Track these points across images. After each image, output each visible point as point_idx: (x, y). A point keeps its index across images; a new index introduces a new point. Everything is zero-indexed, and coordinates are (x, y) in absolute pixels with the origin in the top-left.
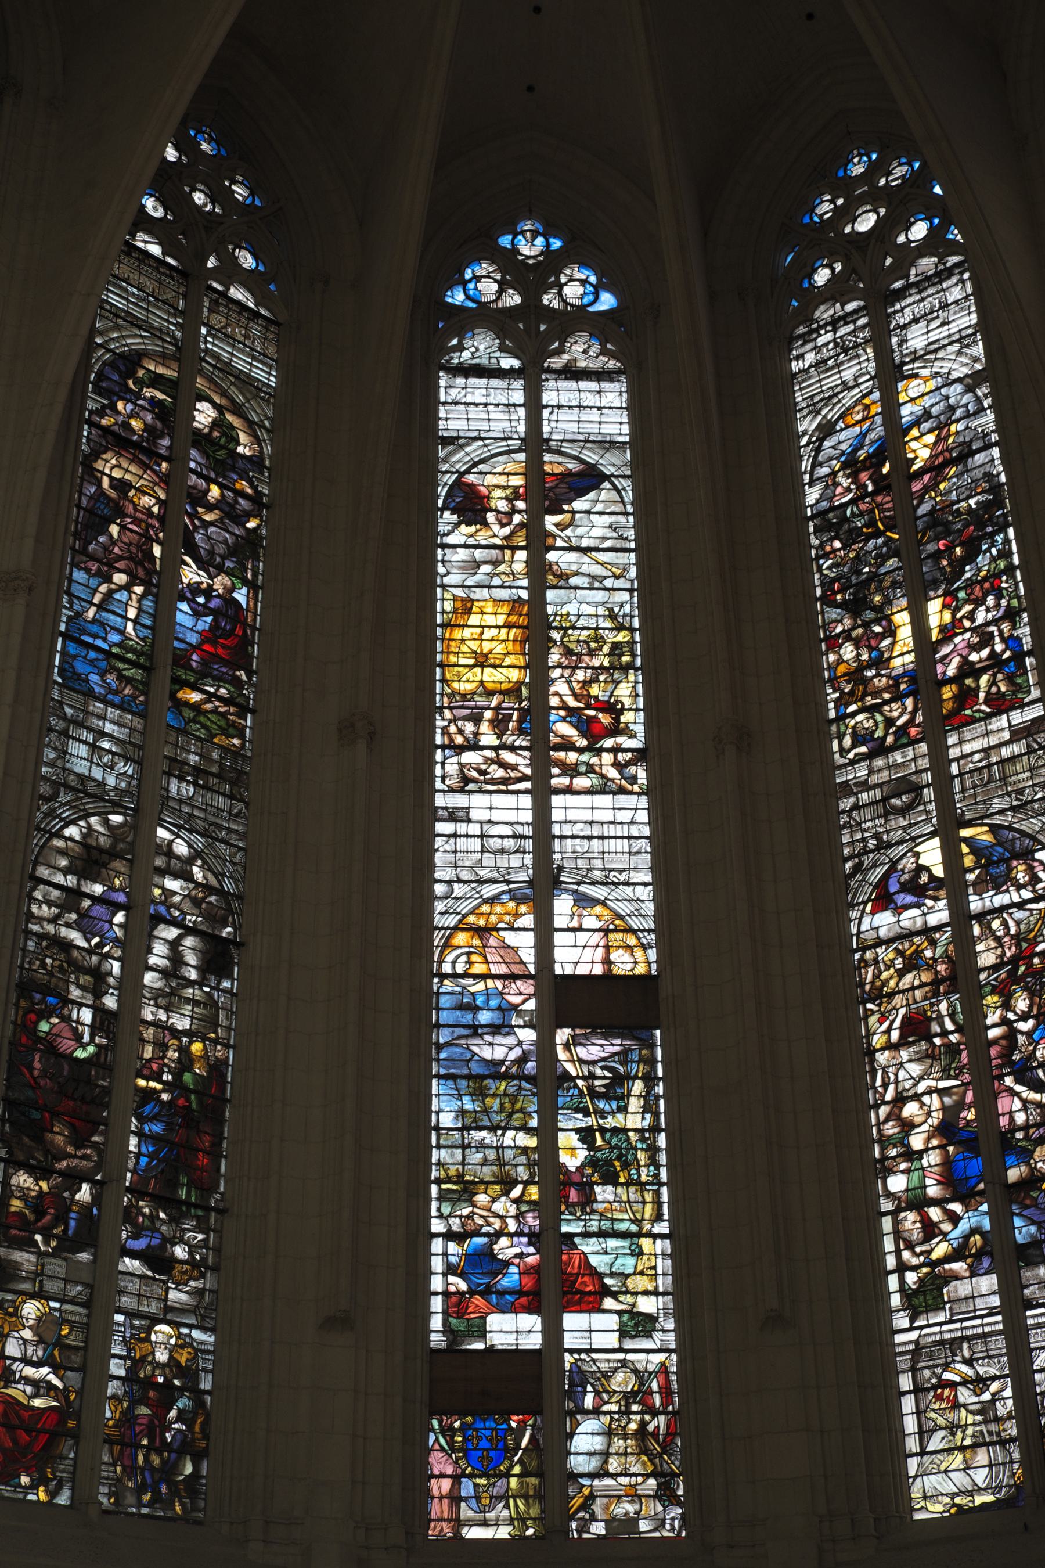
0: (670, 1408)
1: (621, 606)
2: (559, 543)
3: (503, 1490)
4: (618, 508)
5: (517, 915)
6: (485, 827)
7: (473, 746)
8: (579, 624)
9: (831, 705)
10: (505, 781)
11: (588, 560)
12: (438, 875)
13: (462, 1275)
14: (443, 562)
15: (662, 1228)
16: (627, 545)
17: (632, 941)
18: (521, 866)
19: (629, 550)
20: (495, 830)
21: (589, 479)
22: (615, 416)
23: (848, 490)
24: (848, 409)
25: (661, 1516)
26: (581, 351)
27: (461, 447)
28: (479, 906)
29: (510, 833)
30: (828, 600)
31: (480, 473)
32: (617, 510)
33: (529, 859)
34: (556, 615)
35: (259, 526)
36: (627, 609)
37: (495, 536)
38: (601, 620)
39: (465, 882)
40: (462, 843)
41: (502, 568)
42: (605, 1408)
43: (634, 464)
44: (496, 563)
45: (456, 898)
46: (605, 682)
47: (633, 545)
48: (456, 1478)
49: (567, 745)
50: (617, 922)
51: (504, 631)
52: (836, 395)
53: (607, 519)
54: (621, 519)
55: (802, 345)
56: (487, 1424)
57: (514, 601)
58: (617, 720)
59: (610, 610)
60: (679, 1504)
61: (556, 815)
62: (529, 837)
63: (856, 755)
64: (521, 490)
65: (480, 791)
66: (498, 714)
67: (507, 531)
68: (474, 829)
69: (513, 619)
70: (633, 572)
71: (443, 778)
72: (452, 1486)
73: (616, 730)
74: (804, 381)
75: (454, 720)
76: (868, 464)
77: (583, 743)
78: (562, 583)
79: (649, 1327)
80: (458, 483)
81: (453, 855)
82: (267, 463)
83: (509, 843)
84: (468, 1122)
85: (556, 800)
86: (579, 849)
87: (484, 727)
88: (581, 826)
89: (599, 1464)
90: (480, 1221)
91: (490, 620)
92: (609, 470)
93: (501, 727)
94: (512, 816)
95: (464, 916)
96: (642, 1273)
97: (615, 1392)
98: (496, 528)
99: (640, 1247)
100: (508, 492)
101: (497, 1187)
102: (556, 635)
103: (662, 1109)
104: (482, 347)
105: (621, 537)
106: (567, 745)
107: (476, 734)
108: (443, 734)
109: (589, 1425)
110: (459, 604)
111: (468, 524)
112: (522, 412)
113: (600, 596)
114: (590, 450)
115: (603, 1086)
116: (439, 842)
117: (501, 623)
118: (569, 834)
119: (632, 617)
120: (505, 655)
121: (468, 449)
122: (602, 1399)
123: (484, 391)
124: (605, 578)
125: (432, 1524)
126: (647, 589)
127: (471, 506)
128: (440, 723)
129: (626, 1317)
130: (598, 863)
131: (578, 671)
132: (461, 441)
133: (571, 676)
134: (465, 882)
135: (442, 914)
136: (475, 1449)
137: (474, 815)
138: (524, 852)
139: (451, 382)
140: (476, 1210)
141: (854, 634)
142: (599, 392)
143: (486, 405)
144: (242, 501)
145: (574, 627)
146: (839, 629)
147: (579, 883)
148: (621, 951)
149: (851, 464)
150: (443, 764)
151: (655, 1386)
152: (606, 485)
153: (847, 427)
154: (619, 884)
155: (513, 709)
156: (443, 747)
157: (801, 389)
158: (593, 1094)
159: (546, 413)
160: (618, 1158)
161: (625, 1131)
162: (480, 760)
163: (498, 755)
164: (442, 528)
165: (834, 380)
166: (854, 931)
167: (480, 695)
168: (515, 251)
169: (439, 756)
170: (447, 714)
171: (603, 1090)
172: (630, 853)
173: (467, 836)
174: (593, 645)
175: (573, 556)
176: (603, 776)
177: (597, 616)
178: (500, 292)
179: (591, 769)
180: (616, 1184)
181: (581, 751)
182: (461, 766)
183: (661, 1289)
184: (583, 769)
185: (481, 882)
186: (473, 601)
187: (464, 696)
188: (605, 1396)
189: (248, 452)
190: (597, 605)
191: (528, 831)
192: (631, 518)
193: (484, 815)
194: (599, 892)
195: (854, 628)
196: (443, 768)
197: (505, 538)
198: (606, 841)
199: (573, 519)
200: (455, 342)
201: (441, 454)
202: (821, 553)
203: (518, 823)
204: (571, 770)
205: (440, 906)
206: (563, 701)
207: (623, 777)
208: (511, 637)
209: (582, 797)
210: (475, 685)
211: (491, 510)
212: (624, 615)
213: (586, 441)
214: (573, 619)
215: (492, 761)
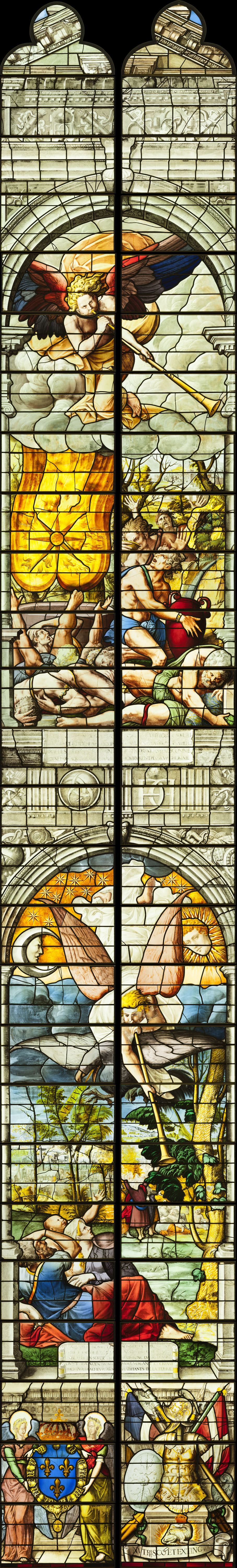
0: (226, 1438)
1: (214, 459)
3: (75, 1518)
4: (216, 303)
6: (61, 773)
11: (175, 388)
13: (35, 1303)
15: (226, 1251)
17: (208, 918)
25: (210, 1542)
39: (38, 846)
40: (34, 796)
42: (161, 1438)
48: (30, 1506)
49: (145, 662)
54: (217, 320)
56: (59, 1453)
58: (202, 624)
60: (228, 1531)
65: (55, 727)
68: (48, 776)
72: (26, 1513)
73: (200, 639)
79: (209, 1356)
80: (28, 267)
84: (41, 1134)
89: (153, 1493)
90: (51, 1244)
92: (205, 242)
95: (37, 889)
96: (204, 1300)
97: (172, 1422)
99: (203, 1273)
101: (71, 1208)
103: (233, 1119)
107: (51, 647)
109: (144, 1455)
111: (41, 336)
113: (188, 444)
115: (172, 1092)
117: (80, 487)
121: (40, 212)
122: (158, 1429)
125: (7, 1549)
129: (185, 1347)
134: (38, 846)
136: (47, 1477)
140: (48, 1233)
148: (195, 932)
151: (211, 1417)
152: (202, 268)
154: (196, 846)
158: (161, 1102)
160: (184, 1175)
161: (191, 1144)
171: (171, 1097)
174: (178, 517)
180: (181, 1203)
182: (34, 692)
183: (222, 1317)
185: (56, 846)
188: (162, 1426)
204: (146, 697)
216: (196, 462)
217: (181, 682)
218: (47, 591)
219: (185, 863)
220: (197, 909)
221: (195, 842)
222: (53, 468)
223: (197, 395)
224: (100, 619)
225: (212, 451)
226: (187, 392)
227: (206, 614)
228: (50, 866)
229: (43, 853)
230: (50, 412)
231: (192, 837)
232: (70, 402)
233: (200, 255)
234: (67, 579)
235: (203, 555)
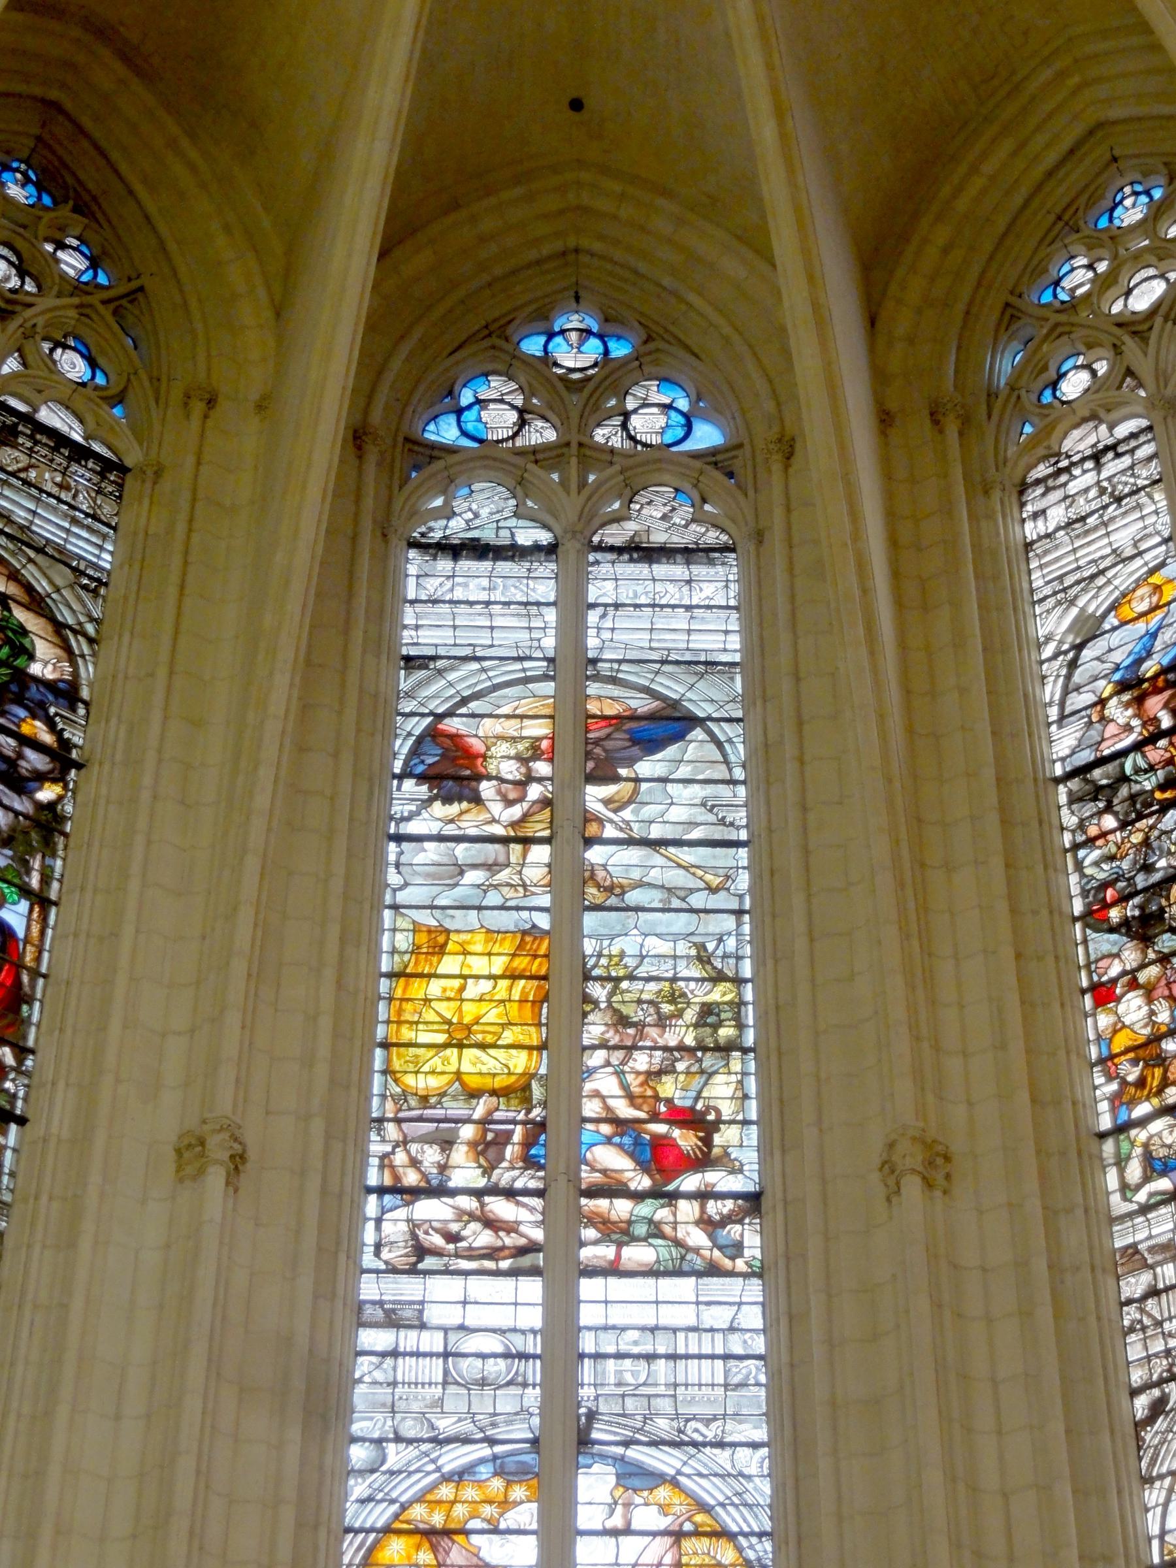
1: (720, 940)
2: (610, 832)
4: (721, 772)
5: (506, 1504)
6: (453, 1337)
7: (438, 1190)
8: (642, 972)
9: (1104, 1106)
10: (493, 1253)
12: (358, 1427)
14: (397, 865)
16: (733, 836)
18: (518, 1412)
19: (737, 844)
20: (472, 1344)
21: (669, 724)
22: (715, 621)
23: (1128, 728)
24: (1124, 595)
26: (658, 515)
27: (440, 672)
28: (434, 1487)
29: (500, 1349)
30: (1094, 918)
31: (473, 716)
32: (716, 776)
33: (533, 1396)
34: (600, 955)
35: (60, 798)
36: (731, 944)
37: (494, 821)
38: (681, 964)
39: (410, 1441)
40: (406, 1368)
41: (504, 876)
43: (747, 699)
44: (492, 867)
45: (392, 1473)
46: (688, 1073)
47: (743, 835)
50: (699, 1518)
51: (504, 984)
52: (1102, 572)
53: (697, 792)
54: (724, 791)
55: (1044, 495)
57: (524, 933)
58: (707, 1142)
59: (701, 947)
61: (588, 1315)
62: (535, 1357)
63: (1151, 1195)
64: (545, 744)
65: (447, 1272)
66: (485, 1131)
67: (516, 811)
68: (432, 1341)
69: (521, 963)
70: (743, 881)
71: (378, 1247)
73: (703, 1161)
74: (1046, 552)
75: (405, 1142)
76: (1160, 682)
77: (643, 1182)
78: (613, 901)
81: (389, 1385)
82: (85, 693)
83: (496, 1368)
85: (589, 1288)
86: (629, 1378)
87: (460, 1155)
88: (633, 1335)
91: (479, 965)
93: (492, 1153)
94: (501, 1317)
95: (404, 1508)
98: (496, 808)
100: (521, 747)
102: (598, 991)
104: (484, 512)
105: (722, 822)
106: (613, 1189)
107: (443, 1168)
108: (382, 1167)
110: (423, 938)
111: (448, 800)
112: (551, 615)
113: (681, 922)
114: (670, 676)
116: (364, 1365)
118: (611, 1349)
119: (739, 958)
120: (504, 1026)
121: (452, 676)
123: (485, 582)
124: (692, 891)
126: (767, 909)
127: (452, 770)
128: (377, 1148)
130: (665, 1405)
131: (636, 1054)
132: (440, 664)
133: (623, 1063)
134: (410, 1441)
135: (363, 1502)
137: (433, 1315)
138: (525, 1385)
139: (427, 568)
141: (1142, 977)
142: (689, 582)
143: (488, 603)
144: (29, 753)
145: (631, 977)
146: (1115, 970)
147: (626, 1444)
149: (1133, 686)
150: (379, 1221)
152: (698, 734)
153: (1124, 623)
154: (704, 1445)
155: (514, 1122)
156: (381, 1191)
157: (1041, 567)
159: (593, 617)
162: (448, 1214)
163: (483, 1205)
164: (397, 809)
165: (1097, 548)
166: (1155, 1530)
167: (455, 1098)
168: (547, 360)
169: (372, 1205)
170: (391, 1130)
172: (726, 1386)
173: (418, 1354)
174: (666, 1008)
175: (633, 855)
176: (678, 1243)
177: (675, 957)
178: (522, 423)
179: (656, 1231)
181: (638, 1197)
182: (414, 1225)
184: (641, 1230)
186: (448, 932)
187: (424, 1100)
189: (49, 674)
190: (675, 938)
191: (533, 1345)
192: (741, 791)
193: (452, 1316)
194: (664, 1461)
195: (1143, 966)
196: (378, 1228)
197: (514, 825)
198: (681, 1364)
199: (636, 792)
200: (438, 502)
201: (403, 686)
202: (1080, 838)
203: (514, 1330)
205: (358, 1488)
206: (608, 1108)
207: (716, 1245)
208: (516, 995)
209: (639, 1281)
210: (445, 1079)
211: (489, 778)
212: (725, 956)
213: (663, 662)
214: (631, 962)
215: (472, 1217)
216: (695, 944)
217: (675, 1215)
218: (443, 1094)
219: (686, 1470)
220: (705, 1541)
221: (700, 1439)
222: (458, 948)
223: (692, 870)
224: (535, 1130)
225: (718, 931)
226: (679, 866)
227: (715, 1126)
228: (428, 1473)
229: (417, 1452)
230: (456, 885)
231: (696, 1430)
232: (488, 874)
233: (693, 721)
234: (473, 1082)
235: (709, 1054)
